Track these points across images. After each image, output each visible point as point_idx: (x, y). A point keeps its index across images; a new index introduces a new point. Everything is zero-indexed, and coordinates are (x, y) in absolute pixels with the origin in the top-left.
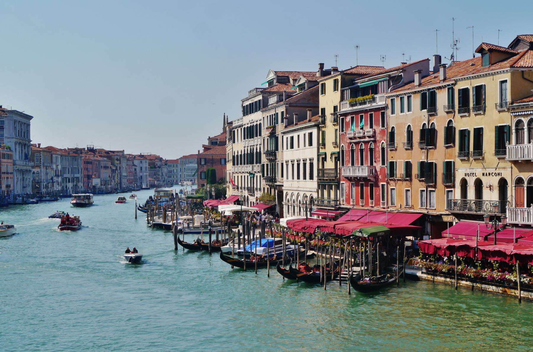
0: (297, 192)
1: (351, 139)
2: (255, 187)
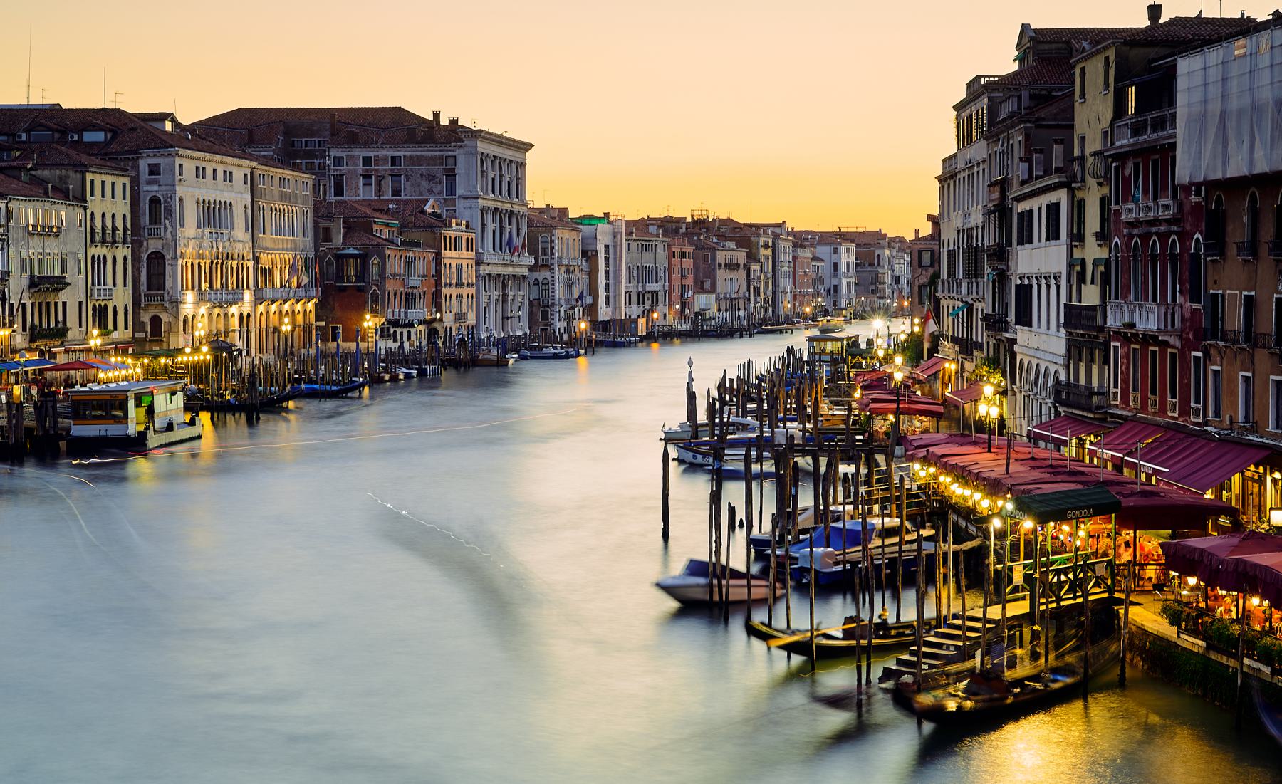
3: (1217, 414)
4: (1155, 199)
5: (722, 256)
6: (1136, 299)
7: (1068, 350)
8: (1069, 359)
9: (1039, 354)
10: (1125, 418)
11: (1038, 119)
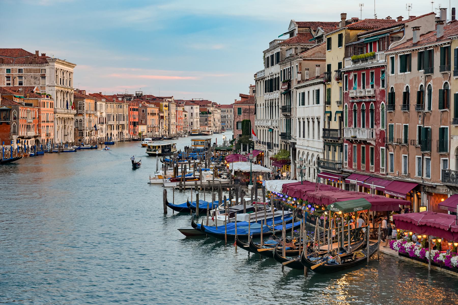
0: (307, 151)
1: (353, 98)
2: (274, 143)
3: (392, 170)
4: (364, 88)
5: (149, 110)
6: (355, 126)
7: (324, 147)
8: (324, 150)
9: (309, 148)
10: (351, 173)
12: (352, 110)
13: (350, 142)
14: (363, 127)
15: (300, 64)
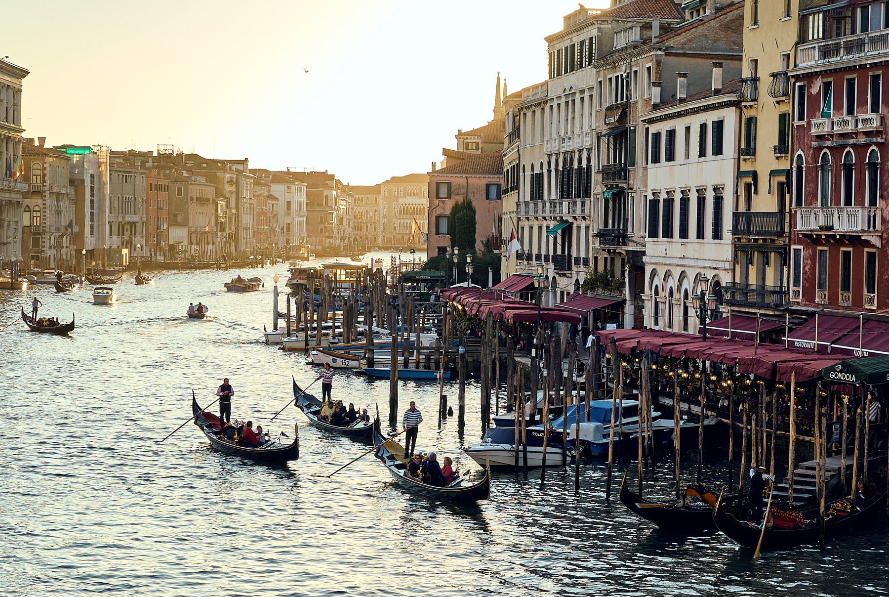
0: (680, 270)
1: (820, 137)
2: (574, 254)
5: (194, 191)
11: (667, 48)
12: (817, 167)
13: (811, 240)
14: (848, 203)
15: (658, 63)
